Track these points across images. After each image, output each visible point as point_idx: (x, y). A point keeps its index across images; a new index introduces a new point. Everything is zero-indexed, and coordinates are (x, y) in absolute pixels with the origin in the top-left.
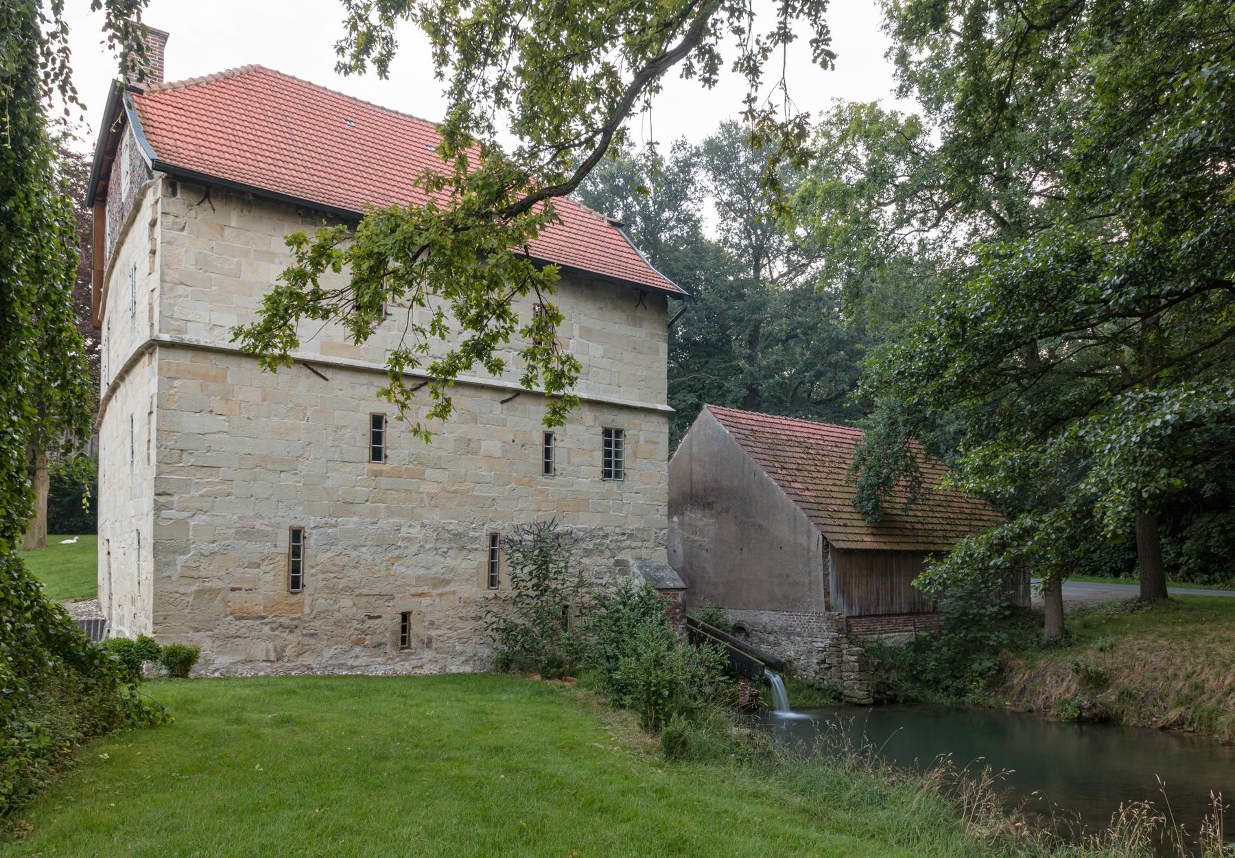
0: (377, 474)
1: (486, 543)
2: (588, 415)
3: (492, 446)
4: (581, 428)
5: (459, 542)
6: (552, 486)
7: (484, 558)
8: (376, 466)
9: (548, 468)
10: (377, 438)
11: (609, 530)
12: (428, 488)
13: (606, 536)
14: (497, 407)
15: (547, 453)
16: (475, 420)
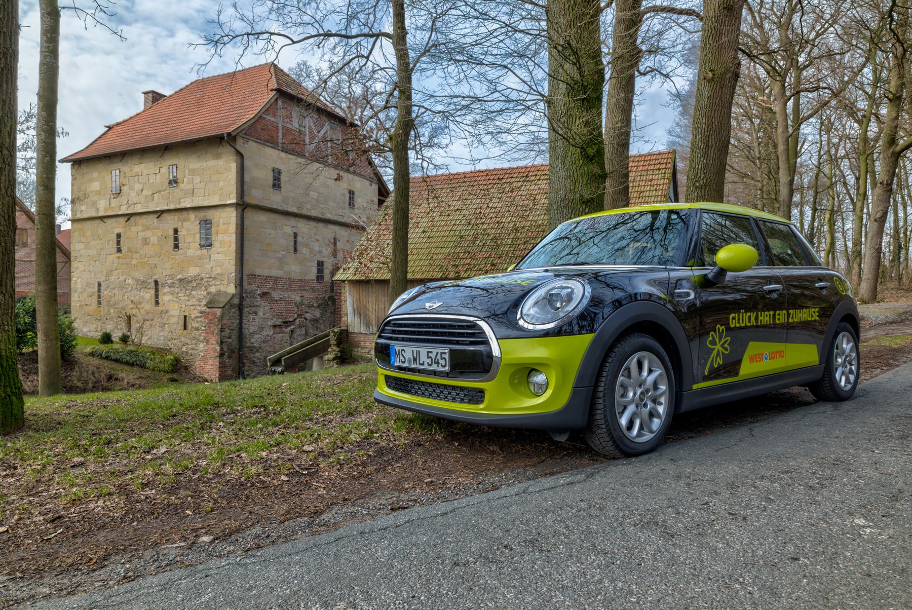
0: (119, 258)
1: (153, 285)
2: (192, 215)
3: (154, 240)
4: (189, 223)
5: (142, 284)
6: (178, 255)
7: (153, 292)
8: (119, 254)
9: (176, 246)
10: (118, 243)
11: (203, 275)
12: (134, 262)
13: (202, 279)
14: (156, 220)
15: (176, 239)
16: (148, 229)
